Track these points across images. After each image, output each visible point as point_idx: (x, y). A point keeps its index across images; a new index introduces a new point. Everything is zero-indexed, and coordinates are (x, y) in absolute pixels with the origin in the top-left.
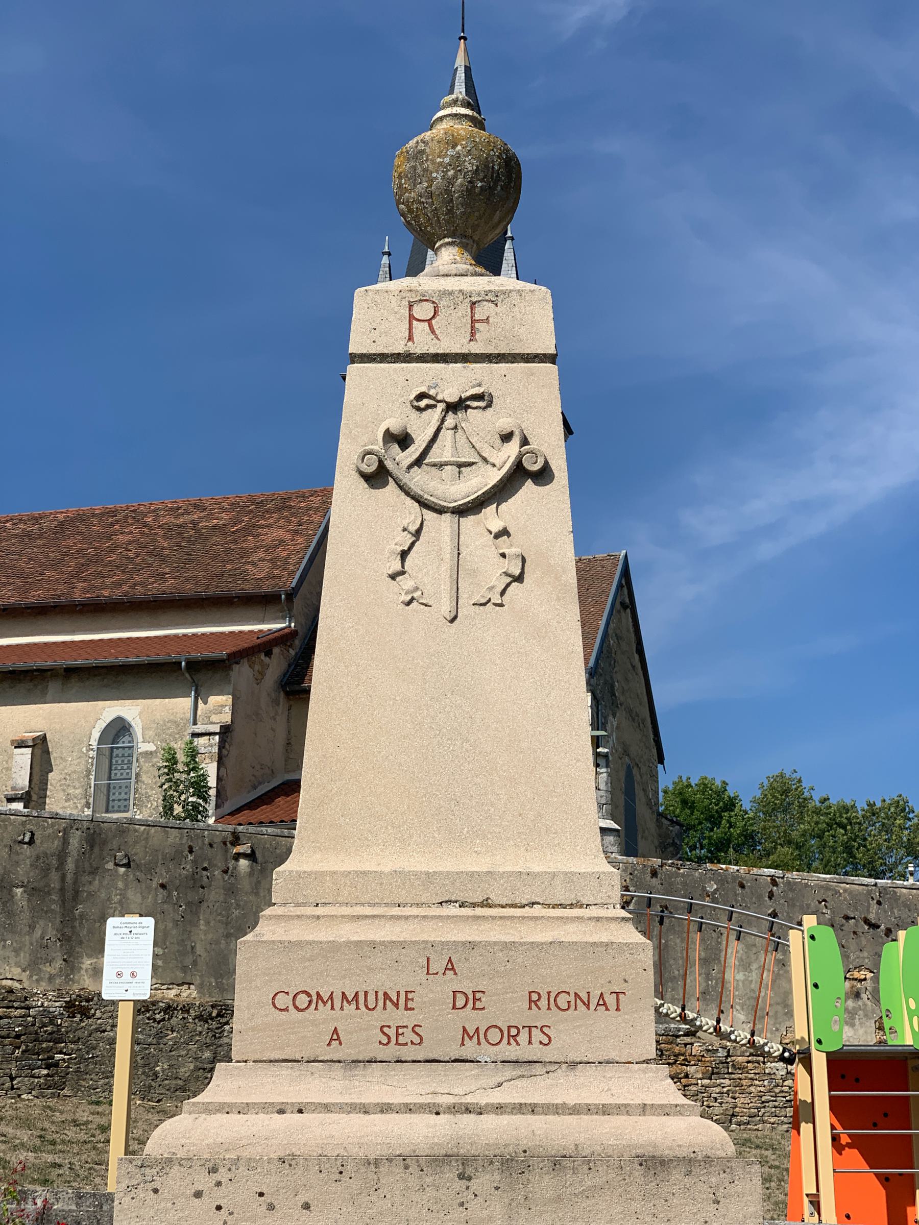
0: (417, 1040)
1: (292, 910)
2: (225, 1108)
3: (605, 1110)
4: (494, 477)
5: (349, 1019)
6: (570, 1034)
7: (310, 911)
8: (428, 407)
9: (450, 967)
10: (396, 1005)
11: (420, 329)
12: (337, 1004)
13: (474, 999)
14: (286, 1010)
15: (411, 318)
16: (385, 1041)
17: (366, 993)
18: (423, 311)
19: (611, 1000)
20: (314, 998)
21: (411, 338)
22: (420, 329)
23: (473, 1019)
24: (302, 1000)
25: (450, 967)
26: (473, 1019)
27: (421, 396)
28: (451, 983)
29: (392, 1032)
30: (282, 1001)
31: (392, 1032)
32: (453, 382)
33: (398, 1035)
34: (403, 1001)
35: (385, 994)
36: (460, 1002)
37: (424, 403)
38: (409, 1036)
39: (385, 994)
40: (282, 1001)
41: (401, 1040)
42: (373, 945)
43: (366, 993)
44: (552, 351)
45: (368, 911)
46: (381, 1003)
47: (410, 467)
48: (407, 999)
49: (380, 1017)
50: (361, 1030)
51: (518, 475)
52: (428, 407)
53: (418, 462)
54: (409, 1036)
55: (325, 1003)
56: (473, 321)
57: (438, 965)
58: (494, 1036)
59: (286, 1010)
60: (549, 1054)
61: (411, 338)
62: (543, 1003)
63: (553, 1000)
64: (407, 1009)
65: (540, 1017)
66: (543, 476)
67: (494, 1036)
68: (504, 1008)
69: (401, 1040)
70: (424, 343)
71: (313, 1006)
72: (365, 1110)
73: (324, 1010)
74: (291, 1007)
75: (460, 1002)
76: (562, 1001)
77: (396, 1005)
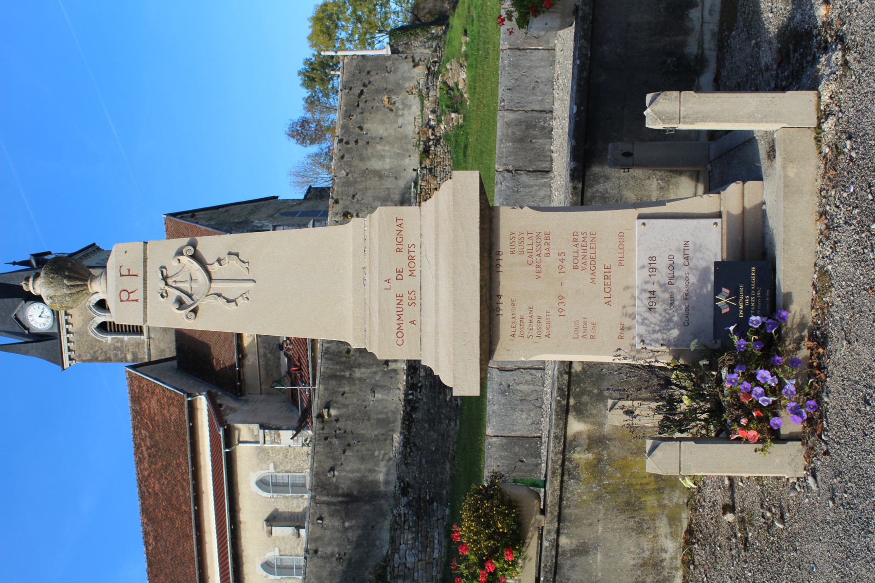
2: (437, 360)
3: (437, 225)
4: (196, 265)
5: (406, 318)
6: (411, 237)
7: (367, 333)
9: (388, 281)
11: (132, 297)
13: (399, 272)
15: (128, 300)
18: (125, 296)
19: (399, 222)
22: (132, 297)
23: (406, 273)
24: (400, 335)
25: (388, 281)
26: (406, 273)
27: (162, 296)
28: (393, 281)
29: (411, 302)
30: (400, 342)
31: (411, 302)
32: (156, 283)
34: (400, 297)
36: (400, 277)
37: (165, 294)
38: (412, 296)
40: (400, 342)
42: (379, 311)
44: (142, 243)
45: (368, 312)
50: (409, 313)
51: (196, 257)
53: (190, 296)
54: (412, 296)
56: (129, 275)
57: (387, 285)
58: (412, 265)
60: (418, 244)
63: (400, 243)
65: (405, 248)
66: (194, 245)
67: (412, 265)
68: (402, 261)
70: (139, 295)
72: (437, 311)
75: (400, 277)
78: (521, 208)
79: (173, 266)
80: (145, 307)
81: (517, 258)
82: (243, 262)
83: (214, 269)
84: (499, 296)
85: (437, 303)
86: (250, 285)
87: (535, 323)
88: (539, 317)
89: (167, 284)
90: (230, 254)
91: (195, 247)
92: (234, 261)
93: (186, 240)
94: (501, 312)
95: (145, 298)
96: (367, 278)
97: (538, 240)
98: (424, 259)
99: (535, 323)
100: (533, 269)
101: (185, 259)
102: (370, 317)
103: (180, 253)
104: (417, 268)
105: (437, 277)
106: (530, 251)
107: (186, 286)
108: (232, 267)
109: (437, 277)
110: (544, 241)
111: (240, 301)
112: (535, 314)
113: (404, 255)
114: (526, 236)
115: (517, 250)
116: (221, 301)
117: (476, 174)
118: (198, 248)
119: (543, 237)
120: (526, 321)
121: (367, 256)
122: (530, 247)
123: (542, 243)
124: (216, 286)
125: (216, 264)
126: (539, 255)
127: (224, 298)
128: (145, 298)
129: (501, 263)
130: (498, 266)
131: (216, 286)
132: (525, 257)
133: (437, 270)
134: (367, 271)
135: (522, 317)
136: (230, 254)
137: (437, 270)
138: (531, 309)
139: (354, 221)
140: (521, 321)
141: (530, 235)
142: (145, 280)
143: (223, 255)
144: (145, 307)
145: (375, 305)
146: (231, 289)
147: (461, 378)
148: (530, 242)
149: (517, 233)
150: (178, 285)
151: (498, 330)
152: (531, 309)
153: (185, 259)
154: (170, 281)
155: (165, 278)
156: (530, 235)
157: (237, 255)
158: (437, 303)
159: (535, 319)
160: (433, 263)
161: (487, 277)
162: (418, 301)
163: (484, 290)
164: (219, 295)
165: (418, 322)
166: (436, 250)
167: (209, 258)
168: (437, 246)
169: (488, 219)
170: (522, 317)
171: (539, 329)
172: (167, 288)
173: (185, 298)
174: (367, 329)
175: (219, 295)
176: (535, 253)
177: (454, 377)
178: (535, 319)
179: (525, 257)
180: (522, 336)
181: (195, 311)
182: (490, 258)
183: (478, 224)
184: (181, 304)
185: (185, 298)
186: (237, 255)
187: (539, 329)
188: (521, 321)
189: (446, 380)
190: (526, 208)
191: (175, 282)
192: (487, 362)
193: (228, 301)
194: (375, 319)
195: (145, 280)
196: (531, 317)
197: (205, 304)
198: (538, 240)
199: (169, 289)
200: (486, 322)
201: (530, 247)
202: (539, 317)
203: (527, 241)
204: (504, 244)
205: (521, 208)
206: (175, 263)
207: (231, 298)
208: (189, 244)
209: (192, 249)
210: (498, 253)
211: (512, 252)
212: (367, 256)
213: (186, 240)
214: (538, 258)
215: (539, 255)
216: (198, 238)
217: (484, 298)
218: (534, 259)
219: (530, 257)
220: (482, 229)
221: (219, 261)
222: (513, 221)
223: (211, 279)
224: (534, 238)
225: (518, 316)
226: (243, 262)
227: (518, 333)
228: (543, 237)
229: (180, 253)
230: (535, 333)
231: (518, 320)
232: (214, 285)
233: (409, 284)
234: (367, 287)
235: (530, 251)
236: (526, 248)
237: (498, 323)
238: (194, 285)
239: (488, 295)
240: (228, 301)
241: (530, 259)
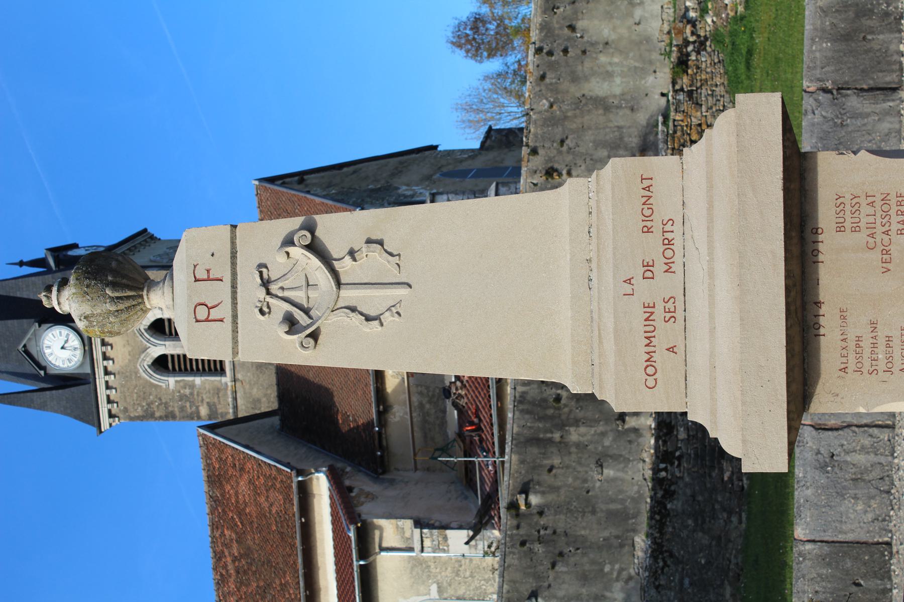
0: (672, 300)
1: (596, 382)
2: (713, 413)
3: (710, 187)
4: (315, 262)
5: (661, 342)
6: (666, 206)
7: (596, 369)
8: (269, 307)
9: (629, 281)
10: (652, 313)
11: (214, 314)
12: (652, 349)
13: (648, 266)
14: (656, 380)
15: (207, 320)
16: (673, 319)
17: (645, 332)
18: (202, 313)
19: (646, 183)
20: (648, 363)
21: (221, 320)
22: (214, 314)
23: (659, 268)
24: (650, 370)
25: (629, 281)
26: (659, 268)
27: (262, 312)
28: (638, 280)
29: (668, 315)
30: (651, 383)
31: (668, 315)
33: (669, 312)
34: (649, 308)
35: (646, 320)
36: (649, 274)
37: (265, 309)
38: (670, 305)
39: (646, 320)
40: (651, 383)
41: (672, 310)
42: (616, 331)
43: (645, 332)
44: (229, 227)
45: (596, 333)
46: (651, 323)
47: (310, 317)
48: (649, 307)
49: (659, 323)
50: (665, 334)
51: (315, 248)
52: (269, 307)
53: (306, 311)
54: (670, 305)
55: (652, 357)
56: (209, 279)
57: (628, 288)
58: (669, 253)
59: (656, 380)
60: (678, 220)
61: (221, 320)
62: (649, 224)
63: (647, 218)
64: (654, 307)
67: (669, 253)
68: (653, 246)
69: (672, 310)
70: (224, 311)
71: (653, 364)
72: (712, 330)
73: (656, 357)
74: (655, 377)
75: (649, 274)
76: (647, 212)
77: (652, 313)
78: (855, 153)
79: (278, 263)
80: (235, 331)
81: (849, 239)
82: (391, 254)
83: (345, 266)
84: (818, 304)
85: (712, 317)
86: (403, 292)
87: (881, 347)
88: (889, 339)
89: (268, 293)
90: (369, 241)
91: (312, 233)
92: (376, 255)
93: (298, 221)
94: (822, 331)
95: (235, 317)
96: (594, 276)
97: (886, 208)
98: (689, 244)
99: (881, 347)
100: (876, 256)
101: (296, 252)
102: (601, 342)
103: (289, 241)
104: (678, 258)
105: (711, 274)
106: (871, 226)
107: (299, 296)
108: (373, 263)
109: (711, 274)
110: (895, 208)
111: (387, 318)
112: (881, 334)
113: (655, 240)
114: (863, 201)
115: (848, 225)
116: (357, 319)
117: (776, 98)
118: (317, 233)
119: (893, 202)
120: (866, 344)
121: (594, 240)
122: (871, 219)
123: (893, 212)
124: (349, 295)
125: (348, 258)
126: (886, 233)
127: (362, 314)
128: (235, 317)
129: (821, 247)
130: (816, 252)
131: (349, 295)
132: (862, 237)
133: (711, 260)
134: (594, 265)
135: (859, 339)
136: (369, 241)
137: (711, 260)
138: (874, 325)
139: (572, 186)
140: (858, 346)
141: (870, 199)
142: (234, 287)
143: (358, 243)
144: (235, 331)
145: (609, 323)
146: (372, 300)
147: (754, 440)
148: (871, 211)
149: (849, 196)
150: (286, 294)
151: (819, 361)
152: (874, 325)
153: (296, 252)
154: (274, 288)
155: (266, 284)
156: (870, 199)
157: (381, 243)
158: (712, 317)
159: (881, 342)
160: (704, 249)
161: (797, 271)
162: (679, 314)
163: (793, 294)
164: (353, 309)
165: (680, 349)
166: (710, 229)
167: (335, 248)
168: (711, 220)
169: (798, 173)
170: (859, 339)
171: (889, 359)
172: (268, 299)
173: (299, 315)
174: (596, 362)
175: (353, 309)
176: (880, 229)
177: (744, 441)
178: (881, 342)
179: (862, 237)
180: (859, 371)
181: (314, 336)
182: (802, 239)
183: (779, 184)
184: (292, 324)
185: (299, 315)
186: (381, 243)
187: (889, 359)
188: (858, 346)
189: (730, 446)
190: (863, 153)
191: (282, 288)
192: (800, 417)
193: (368, 319)
194: (609, 345)
195: (234, 287)
196: (875, 338)
197: (329, 324)
198: (886, 208)
199: (272, 301)
200: (797, 348)
201: (871, 219)
202: (889, 339)
203: (865, 209)
204: (826, 215)
205: (855, 153)
206: (281, 258)
207: (373, 313)
208: (302, 228)
209: (309, 235)
210: (815, 231)
211: (840, 229)
212: (594, 240)
213: (298, 221)
214: (886, 238)
215: (886, 233)
216: (318, 218)
217: (793, 308)
218: (878, 240)
219: (872, 236)
220: (786, 190)
221: (352, 253)
222: (839, 175)
223: (339, 284)
224: (878, 204)
225: (851, 337)
226: (391, 254)
227: (852, 366)
228: (893, 202)
229: (289, 241)
230: (882, 365)
231: (852, 344)
232: (345, 293)
233: (664, 285)
234: (595, 292)
235: (871, 226)
236: (864, 220)
237: (818, 350)
238: (313, 294)
239: (799, 303)
240: (368, 319)
241: (871, 240)
